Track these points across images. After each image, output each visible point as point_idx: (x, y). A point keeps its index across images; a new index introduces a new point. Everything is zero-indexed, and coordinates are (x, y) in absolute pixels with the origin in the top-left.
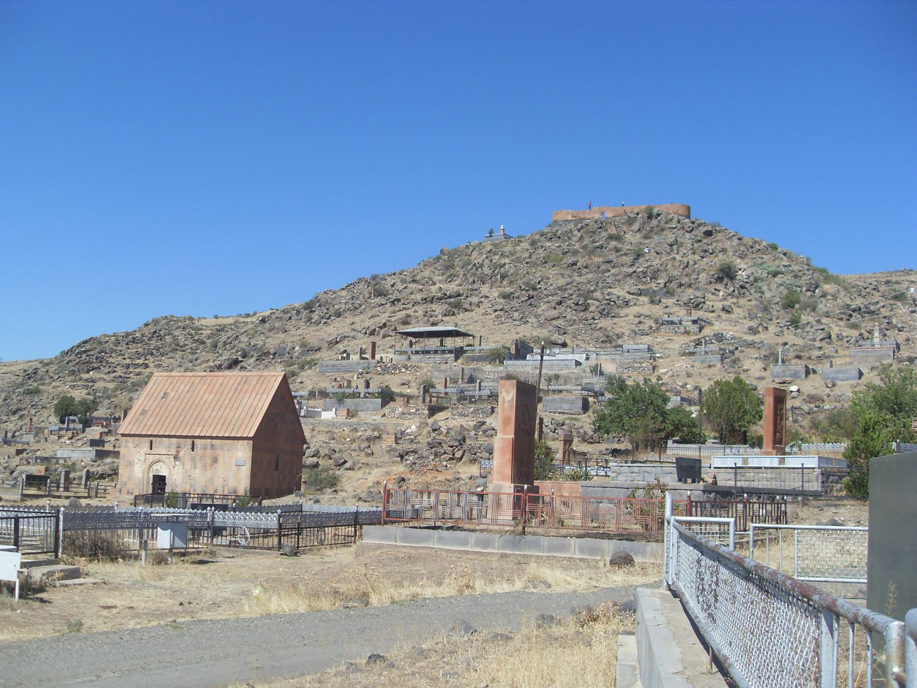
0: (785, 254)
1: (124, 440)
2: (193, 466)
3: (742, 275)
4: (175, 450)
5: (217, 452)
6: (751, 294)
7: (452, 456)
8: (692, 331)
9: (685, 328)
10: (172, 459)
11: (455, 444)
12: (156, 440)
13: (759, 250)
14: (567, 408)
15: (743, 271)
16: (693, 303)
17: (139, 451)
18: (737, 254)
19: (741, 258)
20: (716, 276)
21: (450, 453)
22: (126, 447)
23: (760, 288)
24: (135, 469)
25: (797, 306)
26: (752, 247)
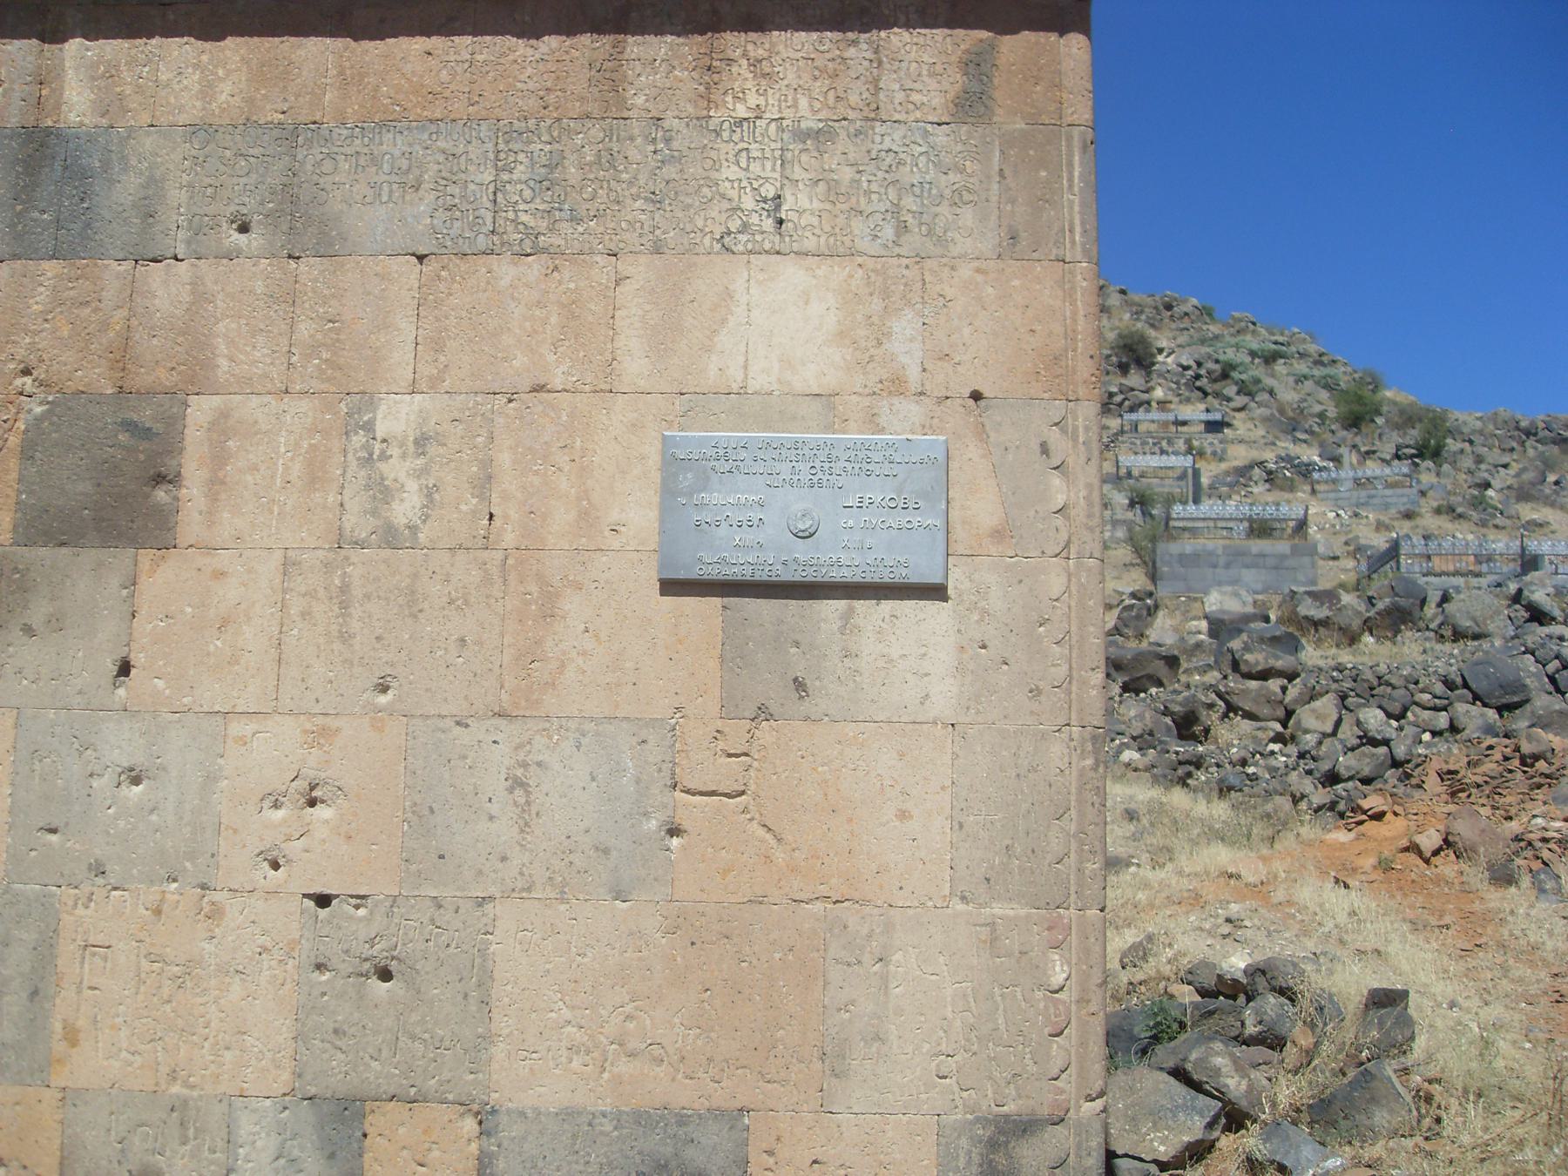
0: (1254, 324)
3: (1166, 362)
6: (1229, 400)
7: (1278, 727)
8: (1209, 451)
9: (1188, 442)
11: (1279, 664)
13: (1186, 314)
14: (1259, 587)
18: (1143, 317)
19: (1152, 326)
20: (1114, 359)
21: (1265, 711)
23: (1257, 381)
25: (1380, 421)
26: (1169, 307)
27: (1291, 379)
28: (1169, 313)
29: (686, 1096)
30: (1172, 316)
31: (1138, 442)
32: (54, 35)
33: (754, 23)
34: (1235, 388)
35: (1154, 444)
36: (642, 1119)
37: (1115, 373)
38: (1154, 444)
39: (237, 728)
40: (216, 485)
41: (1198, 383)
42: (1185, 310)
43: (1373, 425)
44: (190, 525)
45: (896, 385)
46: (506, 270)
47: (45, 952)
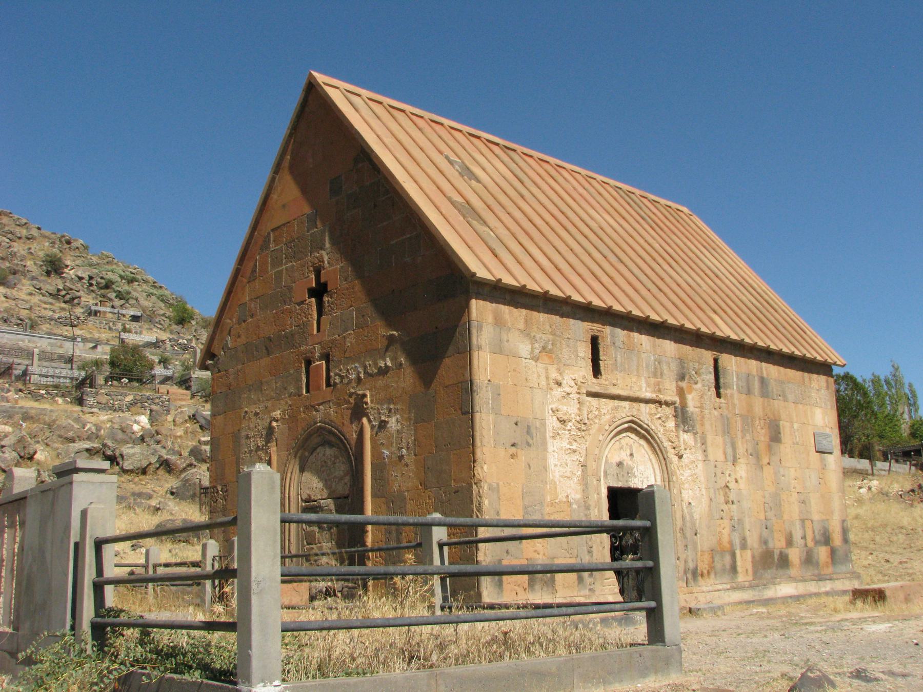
1: (490, 319)
2: (729, 451)
4: (674, 384)
5: (776, 402)
6: (111, 300)
9: (124, 325)
10: (671, 424)
12: (613, 336)
13: (77, 248)
15: (70, 270)
16: (64, 296)
17: (554, 374)
18: (56, 246)
20: (44, 268)
22: (499, 349)
24: (552, 461)
26: (69, 243)
27: (145, 294)
28: (69, 246)
29: (824, 517)
30: (70, 248)
31: (98, 322)
32: (761, 362)
33: (812, 373)
34: (114, 295)
35: (106, 324)
36: (823, 521)
37: (45, 276)
38: (106, 324)
39: (790, 469)
40: (784, 434)
41: (92, 288)
42: (77, 245)
43: (190, 324)
44: (783, 441)
45: (826, 426)
46: (800, 406)
47: (780, 502)
